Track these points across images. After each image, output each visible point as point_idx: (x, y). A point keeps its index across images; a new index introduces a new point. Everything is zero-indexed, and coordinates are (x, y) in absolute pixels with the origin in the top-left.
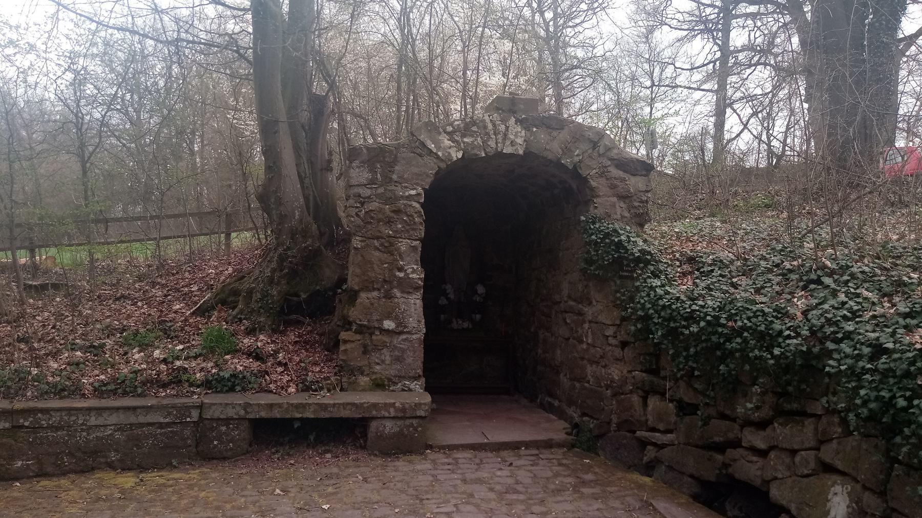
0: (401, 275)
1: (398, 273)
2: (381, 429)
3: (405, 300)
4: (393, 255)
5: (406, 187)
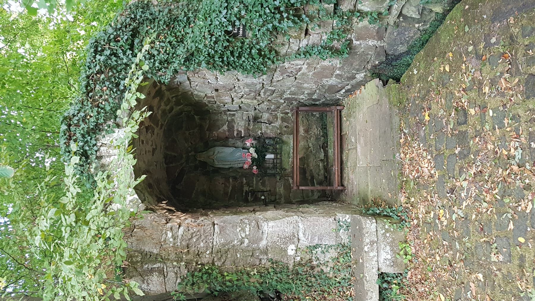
0: (246, 241)
1: (245, 244)
2: (388, 263)
3: (269, 237)
4: (228, 249)
5: (165, 241)
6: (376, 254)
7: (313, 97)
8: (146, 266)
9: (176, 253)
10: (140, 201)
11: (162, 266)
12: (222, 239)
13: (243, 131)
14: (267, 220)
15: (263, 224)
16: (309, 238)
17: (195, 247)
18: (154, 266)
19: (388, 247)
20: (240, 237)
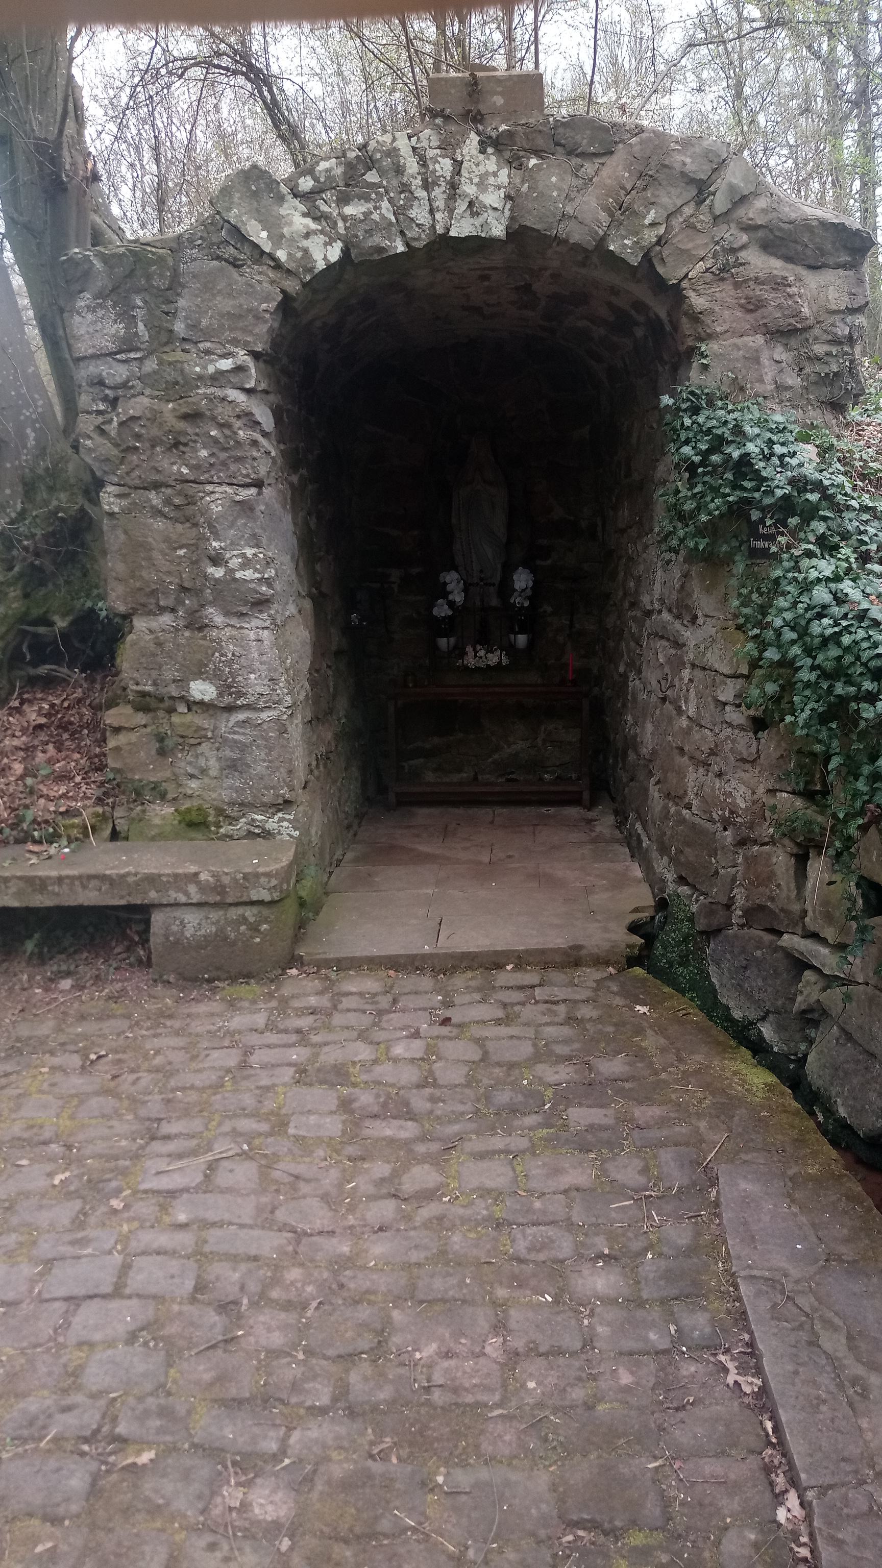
0: (218, 573)
1: (211, 570)
2: (175, 928)
3: (234, 632)
4: (196, 525)
5: (208, 352)
6: (194, 901)
7: (630, 752)
8: (140, 303)
9: (177, 383)
10: (308, 278)
11: (142, 346)
12: (220, 508)
13: (549, 562)
14: (277, 627)
15: (264, 616)
16: (236, 737)
17: (197, 435)
18: (141, 326)
19: (214, 929)
20: (228, 556)
